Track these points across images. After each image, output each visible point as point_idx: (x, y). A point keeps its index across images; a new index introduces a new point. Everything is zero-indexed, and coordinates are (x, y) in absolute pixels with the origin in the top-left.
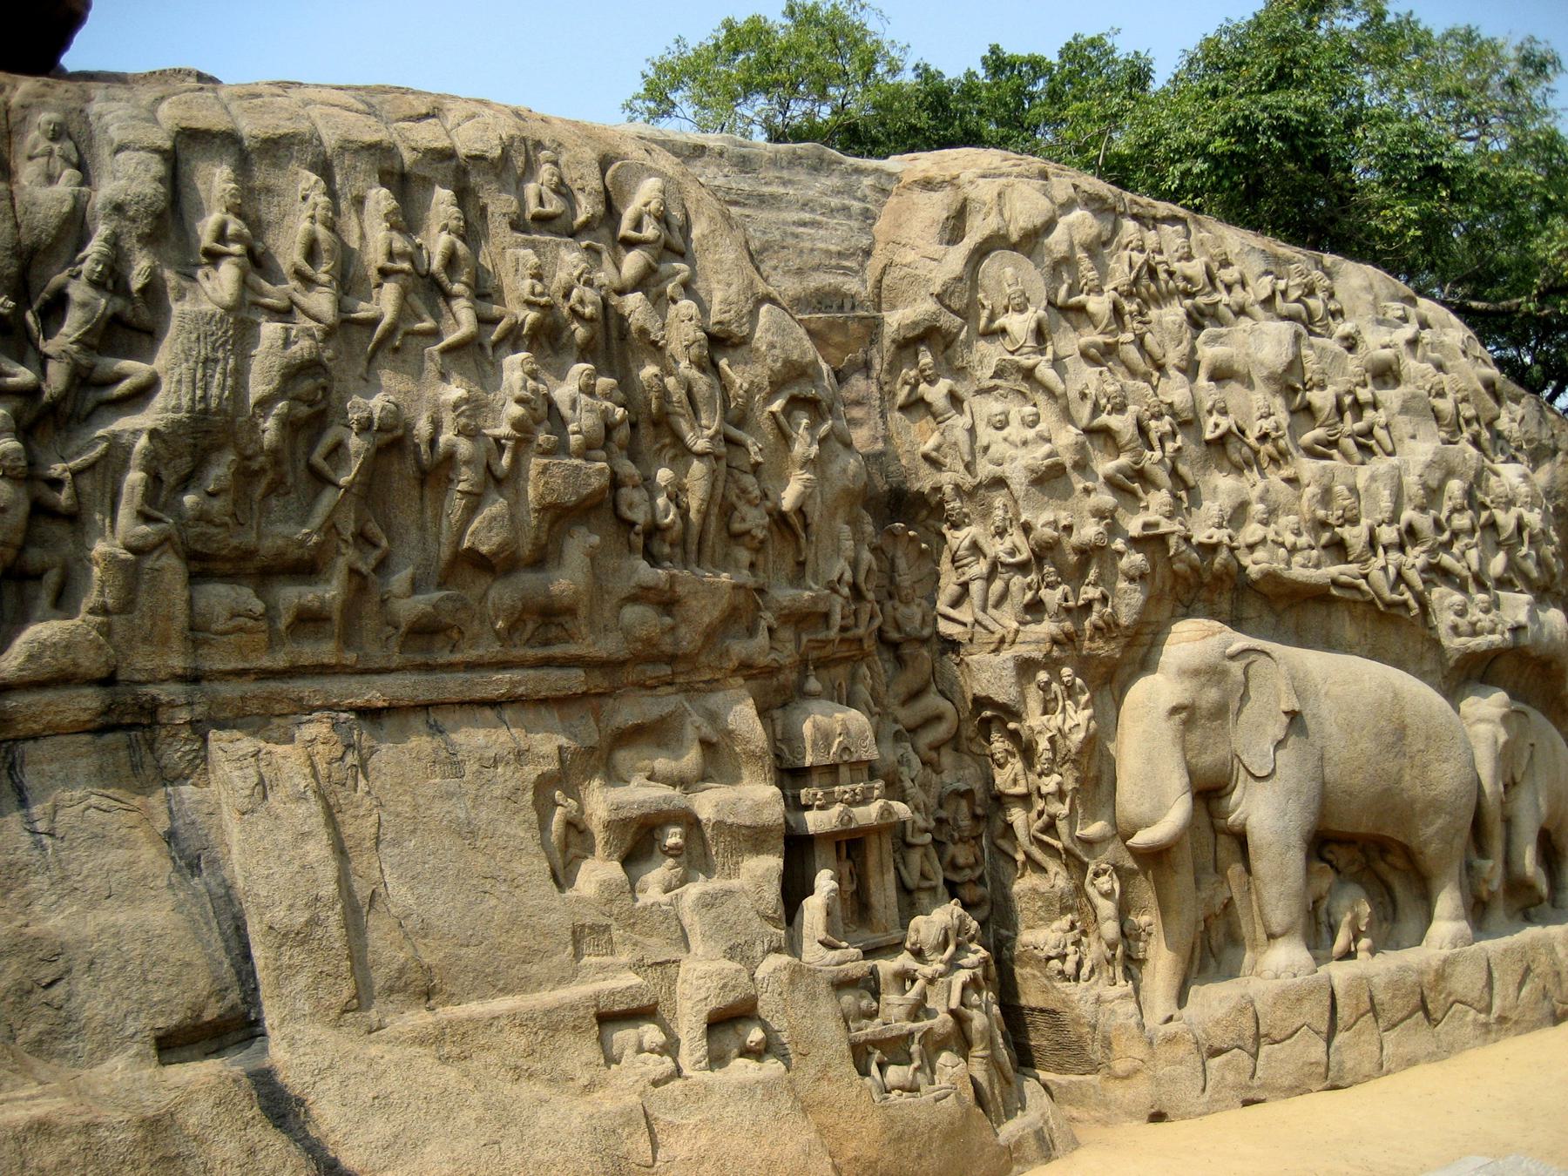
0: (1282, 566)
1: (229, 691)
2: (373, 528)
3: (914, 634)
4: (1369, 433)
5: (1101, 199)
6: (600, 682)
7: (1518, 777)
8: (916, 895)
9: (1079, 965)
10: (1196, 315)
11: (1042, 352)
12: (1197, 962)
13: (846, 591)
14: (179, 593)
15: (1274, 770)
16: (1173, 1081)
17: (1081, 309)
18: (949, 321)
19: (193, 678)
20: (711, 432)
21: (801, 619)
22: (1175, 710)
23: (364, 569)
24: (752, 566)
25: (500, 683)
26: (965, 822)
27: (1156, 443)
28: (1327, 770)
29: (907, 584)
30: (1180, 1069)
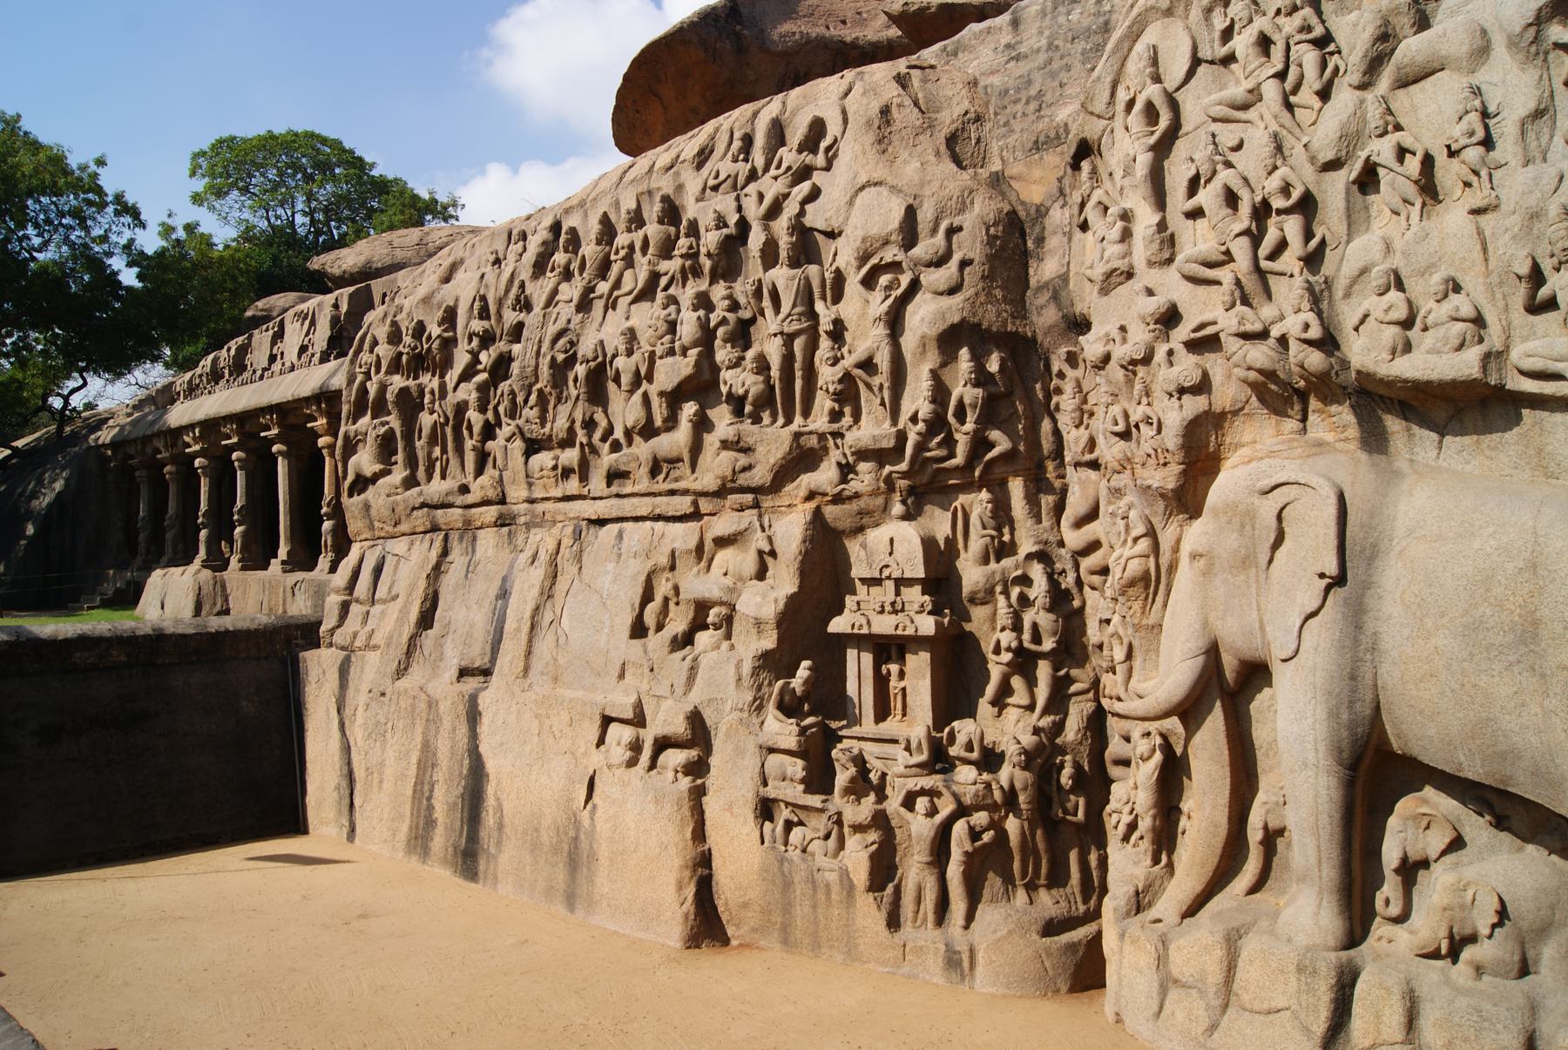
1: (540, 507)
2: (599, 416)
6: (705, 505)
9: (1132, 827)
11: (1152, 133)
13: (921, 426)
14: (521, 460)
15: (1297, 651)
18: (1093, 129)
19: (532, 501)
20: (781, 316)
21: (879, 456)
22: (1194, 556)
23: (585, 441)
24: (835, 416)
25: (643, 506)
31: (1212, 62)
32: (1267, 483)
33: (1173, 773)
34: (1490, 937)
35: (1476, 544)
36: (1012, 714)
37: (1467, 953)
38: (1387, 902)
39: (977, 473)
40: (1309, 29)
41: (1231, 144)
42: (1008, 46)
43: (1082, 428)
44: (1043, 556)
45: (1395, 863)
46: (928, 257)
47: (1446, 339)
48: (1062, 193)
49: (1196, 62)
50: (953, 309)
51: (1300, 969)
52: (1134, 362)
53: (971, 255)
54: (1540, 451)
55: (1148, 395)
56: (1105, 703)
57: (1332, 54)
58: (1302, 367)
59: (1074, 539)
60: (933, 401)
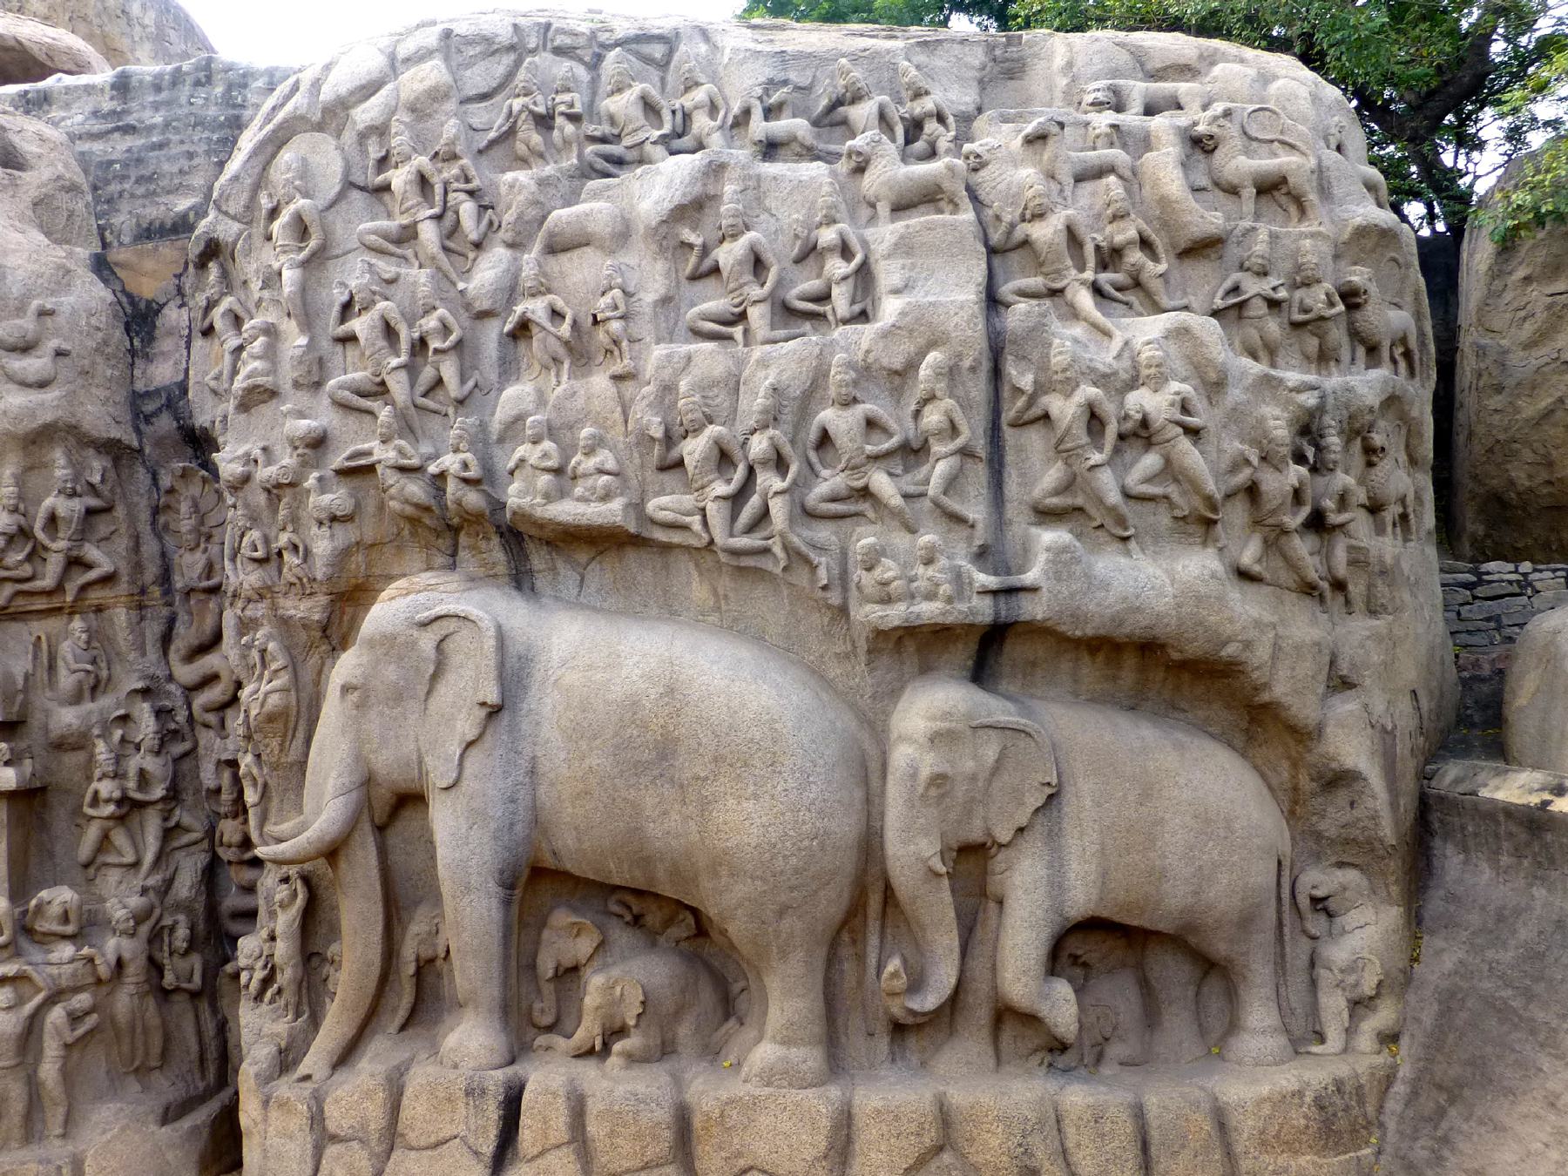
0: (538, 500)
3: (194, 584)
4: (824, 297)
5: (487, 40)
7: (1004, 836)
8: (92, 870)
9: (267, 982)
10: (601, 164)
11: (301, 249)
12: (402, 1013)
16: (279, 1157)
17: (386, 188)
18: (227, 230)
22: (346, 689)
26: (226, 796)
27: (404, 345)
28: (542, 790)
29: (184, 530)
30: (291, 1146)
31: (362, 189)
32: (424, 615)
33: (314, 919)
34: (636, 1026)
35: (624, 673)
36: (113, 876)
37: (617, 1047)
38: (542, 1011)
39: (69, 599)
40: (467, 180)
41: (387, 276)
42: (113, 113)
43: (198, 555)
44: (145, 693)
45: (550, 973)
46: (11, 340)
47: (593, 489)
48: (180, 291)
49: (349, 185)
50: (48, 405)
51: (469, 1093)
52: (279, 486)
53: (66, 346)
54: (665, 592)
55: (293, 521)
56: (220, 851)
57: (486, 208)
58: (460, 505)
59: (187, 673)
60: (15, 510)
